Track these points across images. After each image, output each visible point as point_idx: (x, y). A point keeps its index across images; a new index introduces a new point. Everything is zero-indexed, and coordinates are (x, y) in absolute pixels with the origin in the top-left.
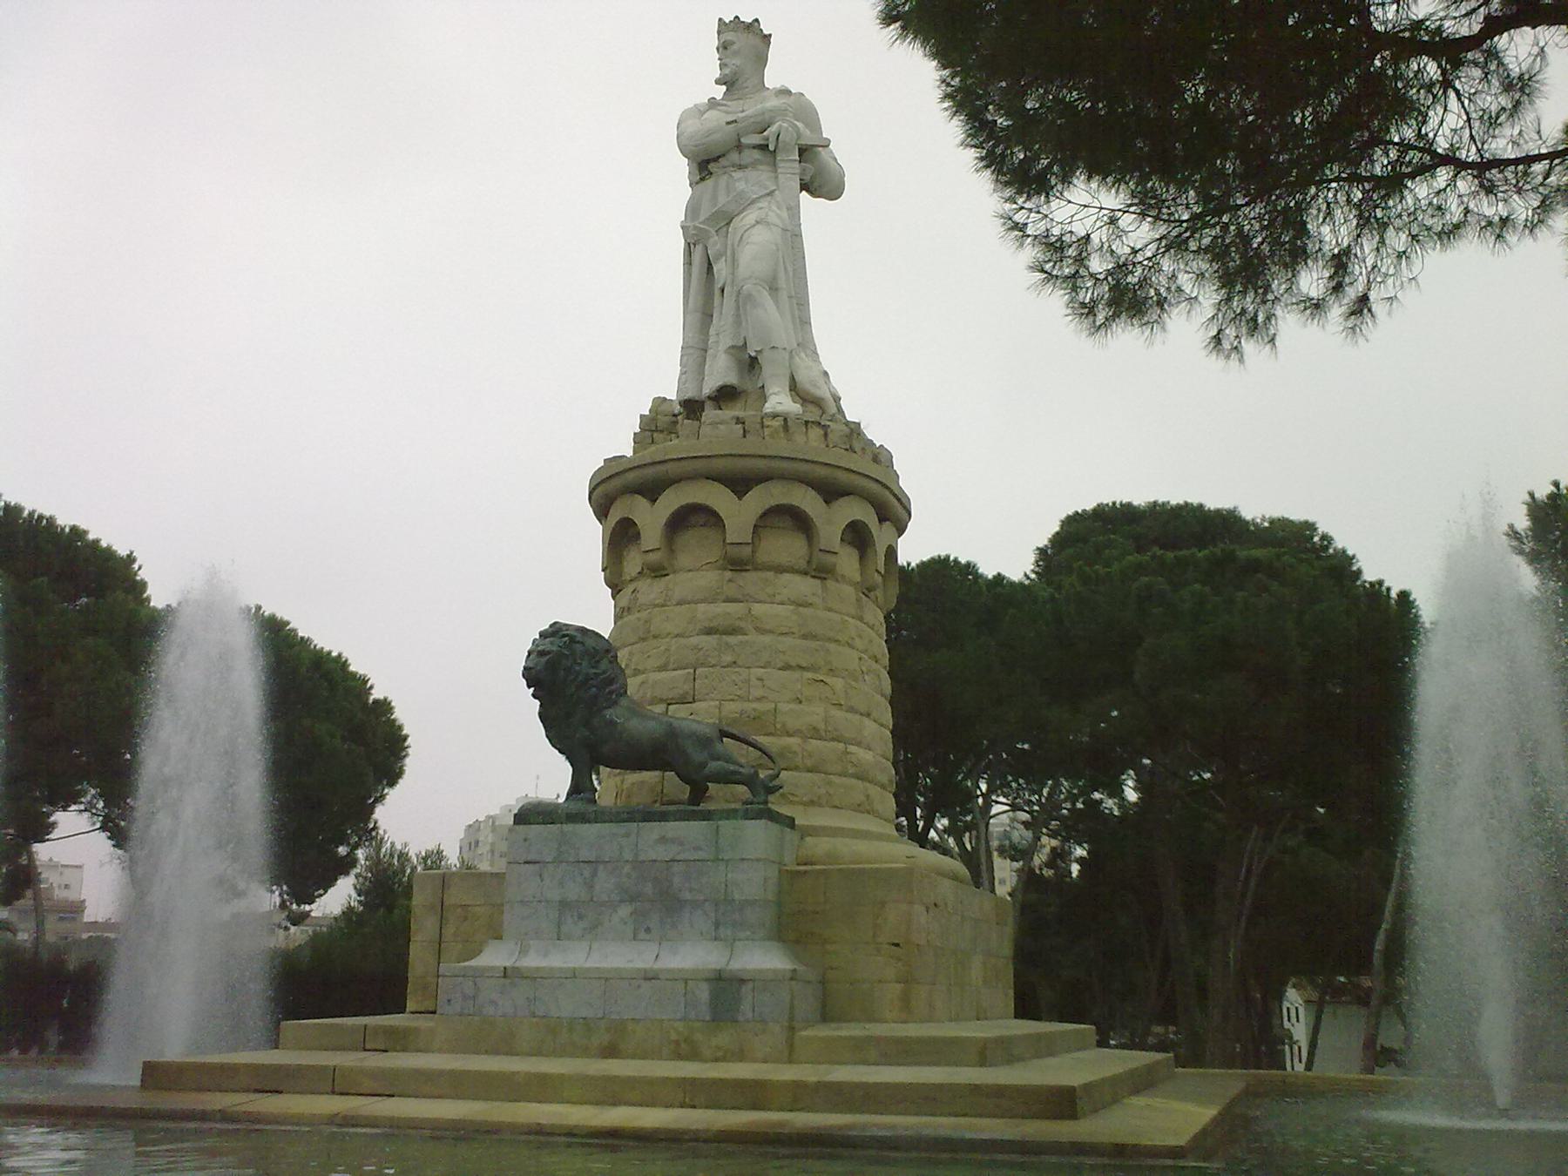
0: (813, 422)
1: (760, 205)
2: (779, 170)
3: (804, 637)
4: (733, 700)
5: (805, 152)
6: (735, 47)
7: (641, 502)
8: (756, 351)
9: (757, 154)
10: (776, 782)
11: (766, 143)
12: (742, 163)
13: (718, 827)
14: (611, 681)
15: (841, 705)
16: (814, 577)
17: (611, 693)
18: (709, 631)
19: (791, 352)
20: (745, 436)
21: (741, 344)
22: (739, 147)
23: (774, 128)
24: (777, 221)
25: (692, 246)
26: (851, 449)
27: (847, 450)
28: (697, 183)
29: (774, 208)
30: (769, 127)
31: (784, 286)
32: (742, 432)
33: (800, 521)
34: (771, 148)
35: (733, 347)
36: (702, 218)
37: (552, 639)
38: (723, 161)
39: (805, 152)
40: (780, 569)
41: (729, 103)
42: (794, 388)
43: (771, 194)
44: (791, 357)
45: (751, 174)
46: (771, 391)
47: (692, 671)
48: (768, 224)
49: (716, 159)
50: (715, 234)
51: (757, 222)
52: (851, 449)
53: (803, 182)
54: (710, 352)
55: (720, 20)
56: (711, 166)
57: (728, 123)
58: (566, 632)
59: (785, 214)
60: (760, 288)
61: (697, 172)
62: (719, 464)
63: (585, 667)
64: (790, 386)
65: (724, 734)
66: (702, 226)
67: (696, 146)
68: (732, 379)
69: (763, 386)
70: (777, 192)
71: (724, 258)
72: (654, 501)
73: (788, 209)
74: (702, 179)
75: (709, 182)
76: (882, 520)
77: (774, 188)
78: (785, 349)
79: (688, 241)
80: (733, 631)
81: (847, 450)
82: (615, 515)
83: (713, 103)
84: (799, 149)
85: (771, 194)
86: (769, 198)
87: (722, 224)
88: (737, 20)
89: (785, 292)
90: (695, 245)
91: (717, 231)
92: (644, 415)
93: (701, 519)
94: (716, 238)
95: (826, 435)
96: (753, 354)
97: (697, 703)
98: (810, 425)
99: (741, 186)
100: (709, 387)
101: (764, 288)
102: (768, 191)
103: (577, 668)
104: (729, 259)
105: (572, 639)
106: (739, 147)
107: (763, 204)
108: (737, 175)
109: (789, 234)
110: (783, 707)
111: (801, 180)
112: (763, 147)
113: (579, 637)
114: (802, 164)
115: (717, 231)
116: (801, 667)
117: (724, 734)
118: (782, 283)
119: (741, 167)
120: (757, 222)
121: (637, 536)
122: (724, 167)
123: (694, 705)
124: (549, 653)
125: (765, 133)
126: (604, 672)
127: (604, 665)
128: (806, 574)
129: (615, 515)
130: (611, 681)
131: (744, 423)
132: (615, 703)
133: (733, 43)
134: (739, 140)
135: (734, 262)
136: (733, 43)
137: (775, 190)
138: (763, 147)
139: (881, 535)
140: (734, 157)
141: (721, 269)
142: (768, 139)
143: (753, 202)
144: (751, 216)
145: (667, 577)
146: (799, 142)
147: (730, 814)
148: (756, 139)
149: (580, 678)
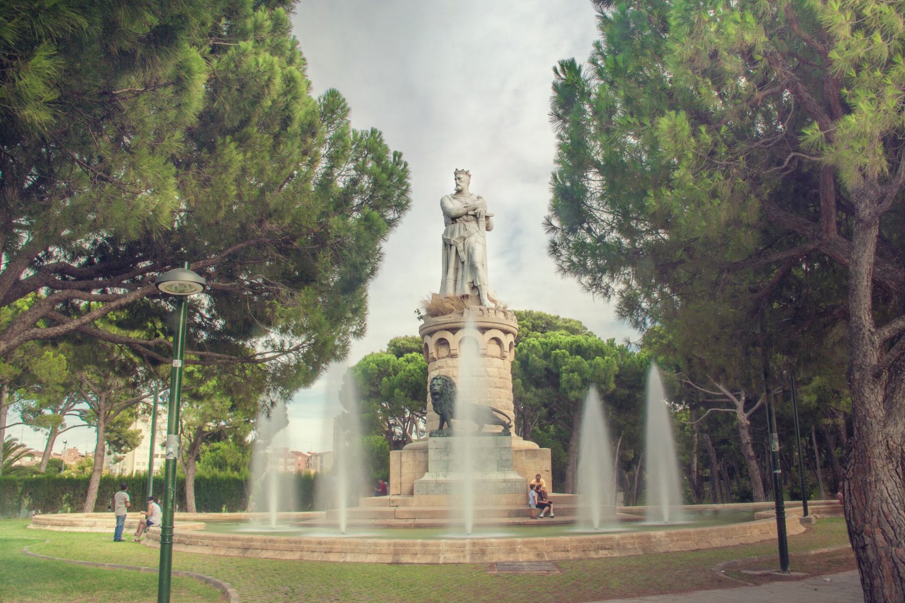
3: (500, 378)
5: (487, 217)
9: (472, 218)
22: (467, 214)
33: (498, 341)
38: (461, 219)
39: (487, 217)
49: (459, 218)
56: (457, 220)
69: (479, 295)
72: (454, 334)
90: (451, 245)
110: (496, 400)
112: (475, 216)
119: (467, 221)
138: (475, 216)
148: (472, 213)
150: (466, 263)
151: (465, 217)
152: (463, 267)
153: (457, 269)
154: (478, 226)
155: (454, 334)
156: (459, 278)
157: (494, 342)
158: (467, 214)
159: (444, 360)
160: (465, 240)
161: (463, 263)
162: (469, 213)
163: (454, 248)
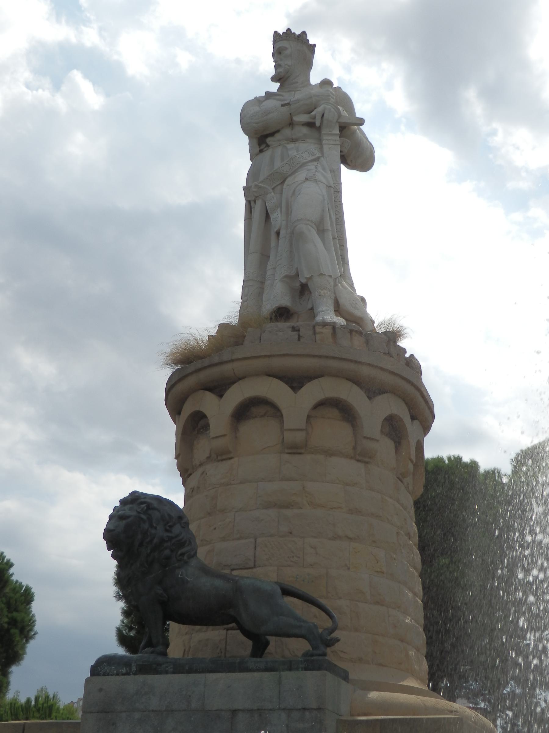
0: (356, 331)
1: (308, 167)
2: (324, 142)
4: (289, 566)
6: (288, 52)
7: (209, 397)
8: (306, 278)
10: (334, 635)
12: (294, 137)
13: (280, 677)
14: (182, 544)
15: (383, 573)
16: (358, 461)
17: (183, 554)
18: (268, 505)
19: (336, 279)
20: (299, 340)
21: (294, 274)
22: (291, 124)
23: (320, 109)
24: (324, 181)
25: (252, 203)
26: (389, 354)
27: (385, 353)
28: (257, 155)
29: (320, 169)
30: (315, 108)
31: (330, 228)
32: (297, 337)
34: (318, 124)
35: (286, 276)
36: (261, 178)
37: (131, 506)
38: (278, 136)
40: (329, 453)
41: (282, 93)
42: (338, 309)
43: (317, 159)
44: (335, 285)
45: (302, 146)
46: (320, 309)
47: (252, 540)
48: (316, 181)
49: (272, 134)
50: (271, 191)
51: (307, 179)
52: (389, 354)
53: (343, 154)
54: (268, 282)
55: (275, 33)
56: (269, 140)
57: (282, 105)
58: (143, 500)
59: (329, 175)
60: (310, 227)
61: (258, 146)
62: (277, 363)
63: (160, 532)
64: (334, 307)
65: (286, 592)
66: (261, 185)
67: (257, 123)
68: (286, 301)
69: (312, 309)
70: (322, 158)
71: (279, 209)
72: (221, 396)
73: (331, 171)
74: (261, 151)
75: (268, 154)
76: (413, 418)
77: (320, 155)
78: (331, 276)
79: (249, 199)
80: (289, 506)
81: (385, 353)
82: (188, 409)
83: (269, 95)
84: (340, 127)
85: (317, 159)
86: (315, 163)
87: (278, 183)
88: (289, 32)
89: (330, 234)
91: (273, 189)
92: (212, 336)
94: (273, 194)
95: (367, 342)
96: (304, 281)
97: (258, 568)
98: (354, 333)
99: (292, 153)
100: (268, 307)
101: (312, 227)
102: (314, 157)
103: (153, 531)
104: (284, 209)
105: (149, 507)
106: (291, 124)
107: (312, 166)
108: (291, 146)
109: (332, 190)
111: (341, 151)
112: (311, 125)
113: (155, 504)
114: (341, 139)
115: (273, 189)
116: (350, 539)
117: (286, 592)
118: (328, 226)
120: (307, 179)
121: (206, 427)
122: (279, 140)
123: (254, 570)
124: (128, 517)
125: (313, 113)
126: (177, 536)
127: (177, 529)
128: (351, 458)
129: (188, 409)
130: (182, 544)
131: (299, 330)
132: (186, 563)
133: (286, 49)
134: (291, 119)
135: (288, 211)
136: (286, 49)
137: (321, 157)
138: (311, 125)
139: (412, 428)
140: (287, 132)
141: (277, 218)
142: (314, 118)
143: (304, 165)
144: (301, 175)
146: (339, 120)
147: (290, 666)
148: (304, 118)
149: (155, 541)
152: (277, 246)
154: (321, 149)
156: (269, 273)
157: (335, 413)
161: (278, 233)
162: (296, 119)
163: (259, 203)
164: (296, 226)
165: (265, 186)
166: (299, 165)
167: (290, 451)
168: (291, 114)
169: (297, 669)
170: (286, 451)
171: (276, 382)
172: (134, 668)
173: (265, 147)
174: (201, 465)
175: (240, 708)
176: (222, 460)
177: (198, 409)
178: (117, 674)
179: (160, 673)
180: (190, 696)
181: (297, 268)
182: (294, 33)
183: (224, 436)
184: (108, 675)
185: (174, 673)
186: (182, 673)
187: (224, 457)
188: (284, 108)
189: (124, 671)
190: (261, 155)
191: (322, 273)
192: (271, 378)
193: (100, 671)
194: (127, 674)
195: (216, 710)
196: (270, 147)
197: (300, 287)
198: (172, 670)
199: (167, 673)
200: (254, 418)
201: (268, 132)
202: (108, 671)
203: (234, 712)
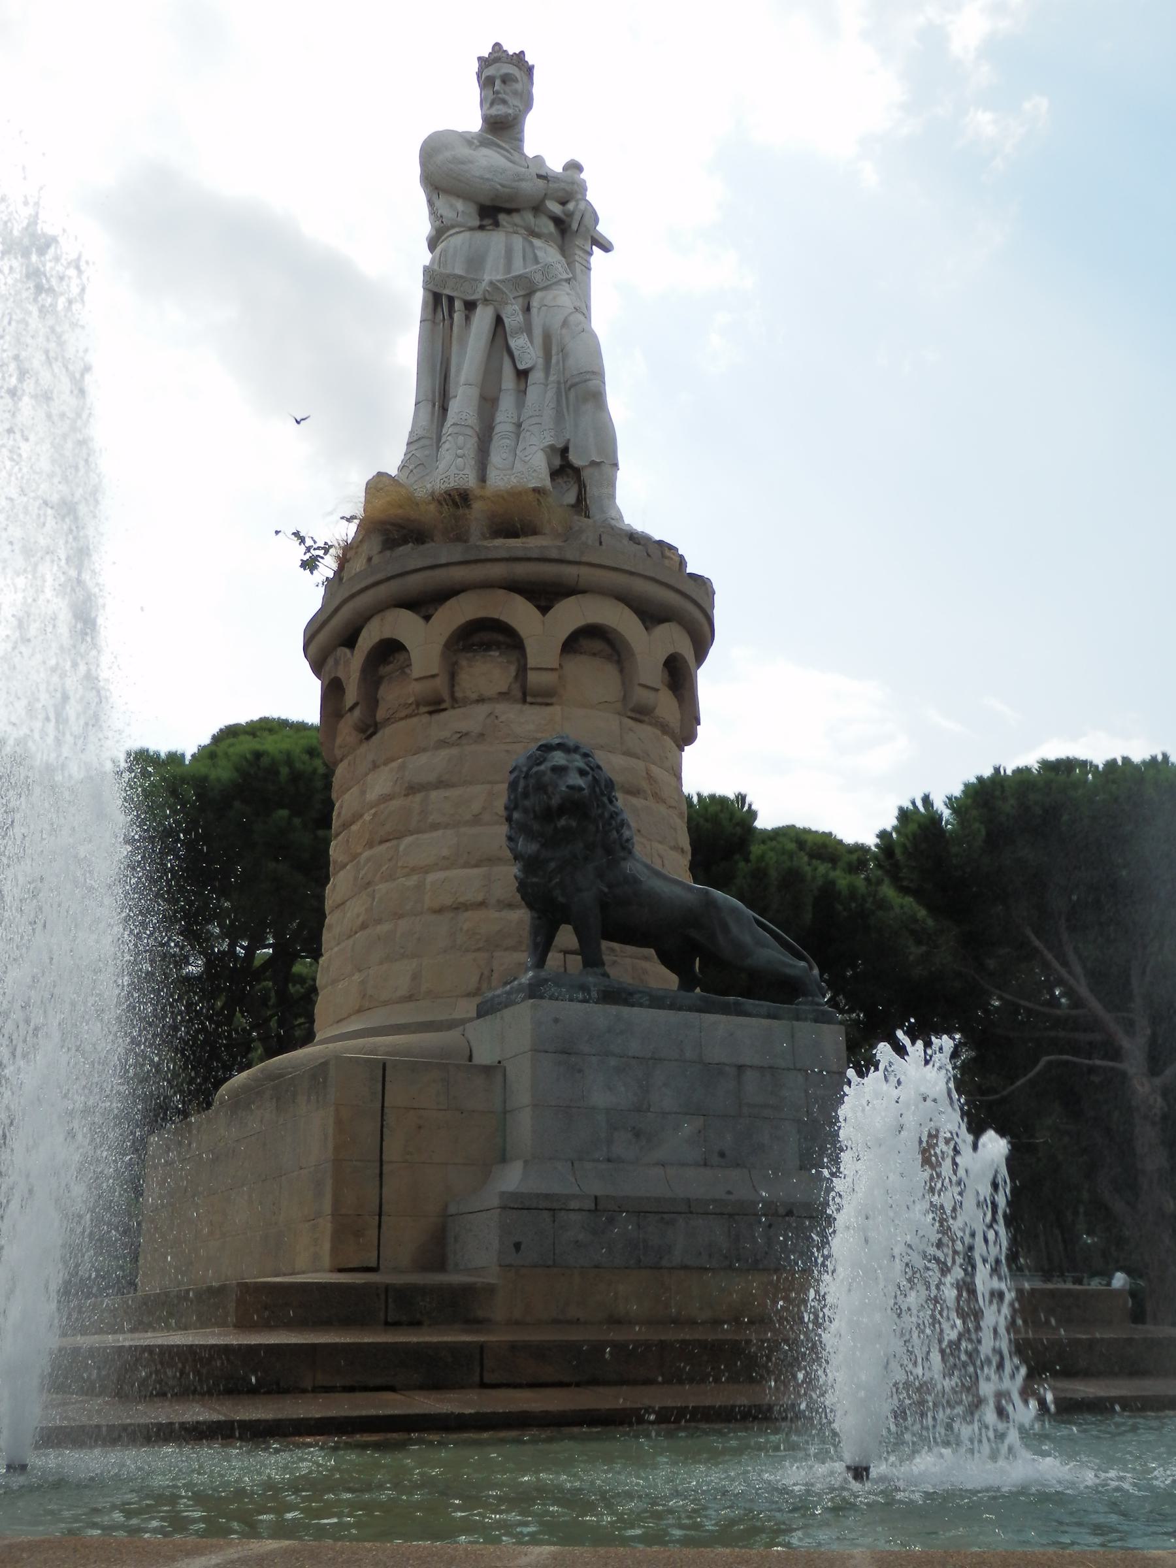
9: (551, 227)
11: (563, 216)
12: (536, 229)
22: (537, 208)
38: (516, 218)
41: (512, 151)
49: (509, 211)
56: (502, 217)
72: (544, 610)
74: (481, 228)
90: (470, 306)
93: (598, 645)
122: (516, 225)
133: (516, 81)
136: (516, 81)
145: (549, 709)
150: (536, 376)
151: (529, 217)
153: (488, 403)
155: (544, 610)
158: (537, 208)
159: (482, 710)
160: (529, 295)
161: (522, 375)
164: (589, 380)
165: (501, 286)
166: (555, 280)
167: (633, 715)
168: (545, 194)
169: (805, 1020)
170: (629, 714)
171: (627, 611)
172: (594, 994)
173: (490, 225)
174: (481, 700)
175: (748, 1063)
176: (532, 704)
177: (496, 616)
178: (571, 1000)
179: (633, 1006)
180: (682, 1042)
181: (569, 440)
182: (527, 62)
183: (552, 669)
184: (557, 999)
185: (650, 1007)
186: (664, 1008)
187: (539, 700)
188: (541, 183)
189: (580, 996)
190: (480, 236)
191: (594, 459)
192: (622, 605)
193: (545, 993)
194: (585, 1001)
195: (717, 1064)
196: (500, 229)
197: (558, 467)
198: (647, 1003)
199: (641, 1005)
200: (581, 653)
201: (507, 205)
202: (556, 994)
203: (741, 1068)
